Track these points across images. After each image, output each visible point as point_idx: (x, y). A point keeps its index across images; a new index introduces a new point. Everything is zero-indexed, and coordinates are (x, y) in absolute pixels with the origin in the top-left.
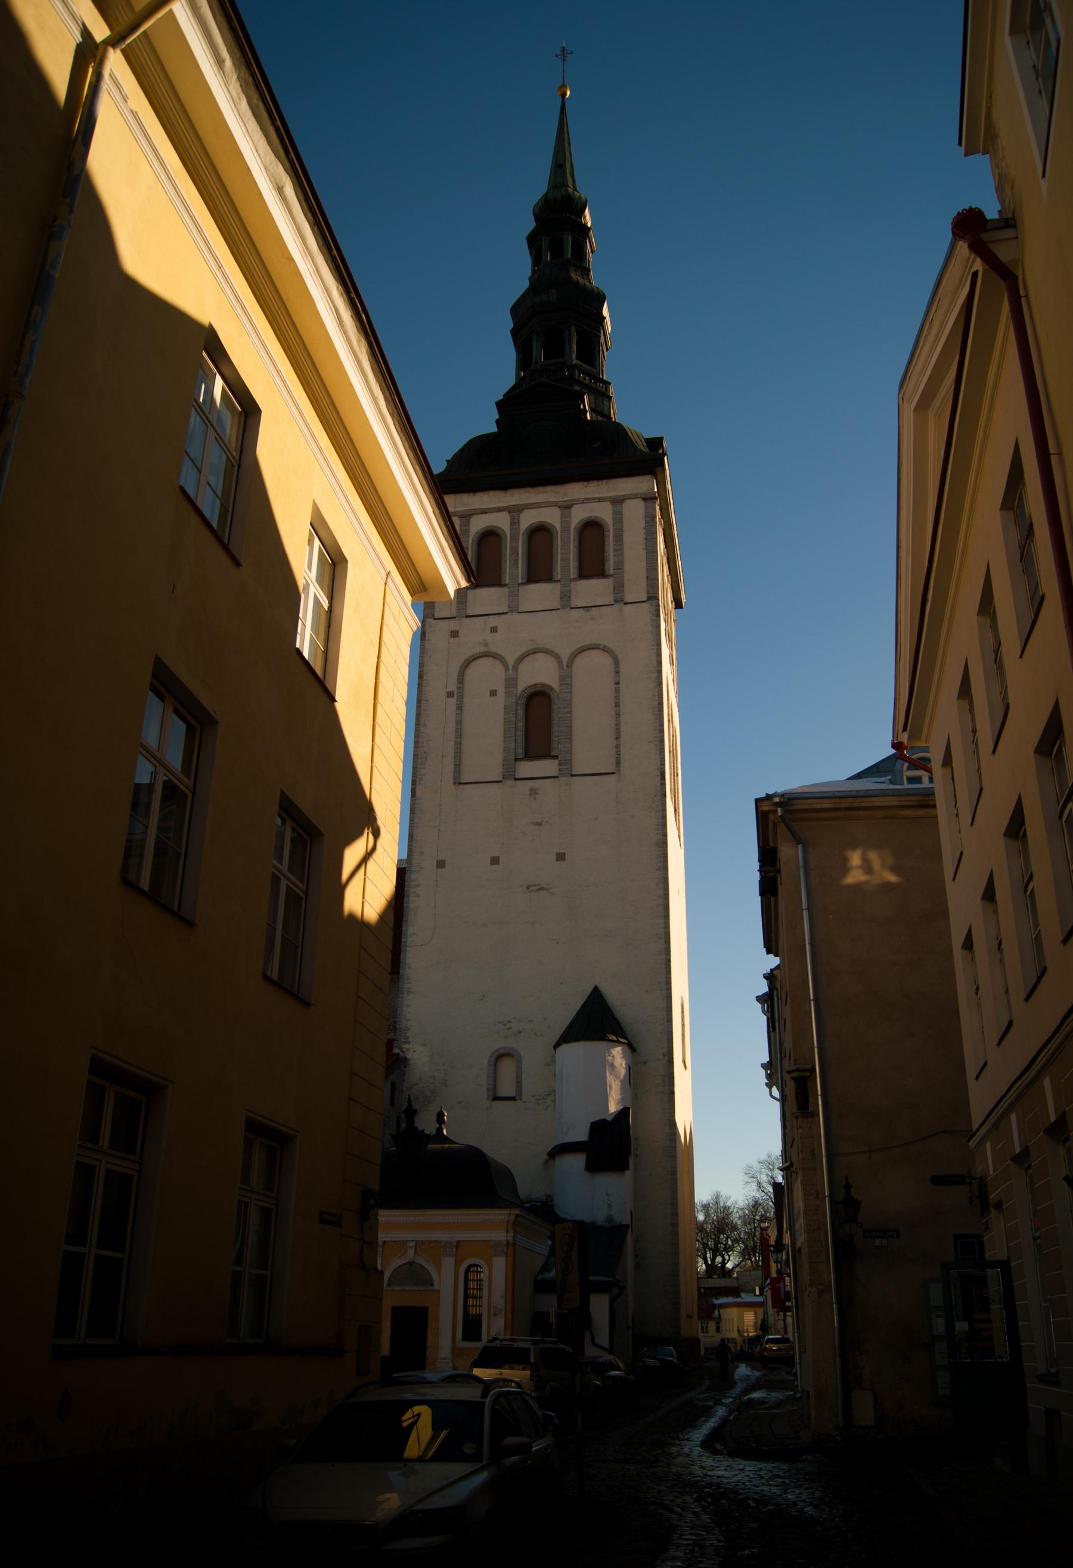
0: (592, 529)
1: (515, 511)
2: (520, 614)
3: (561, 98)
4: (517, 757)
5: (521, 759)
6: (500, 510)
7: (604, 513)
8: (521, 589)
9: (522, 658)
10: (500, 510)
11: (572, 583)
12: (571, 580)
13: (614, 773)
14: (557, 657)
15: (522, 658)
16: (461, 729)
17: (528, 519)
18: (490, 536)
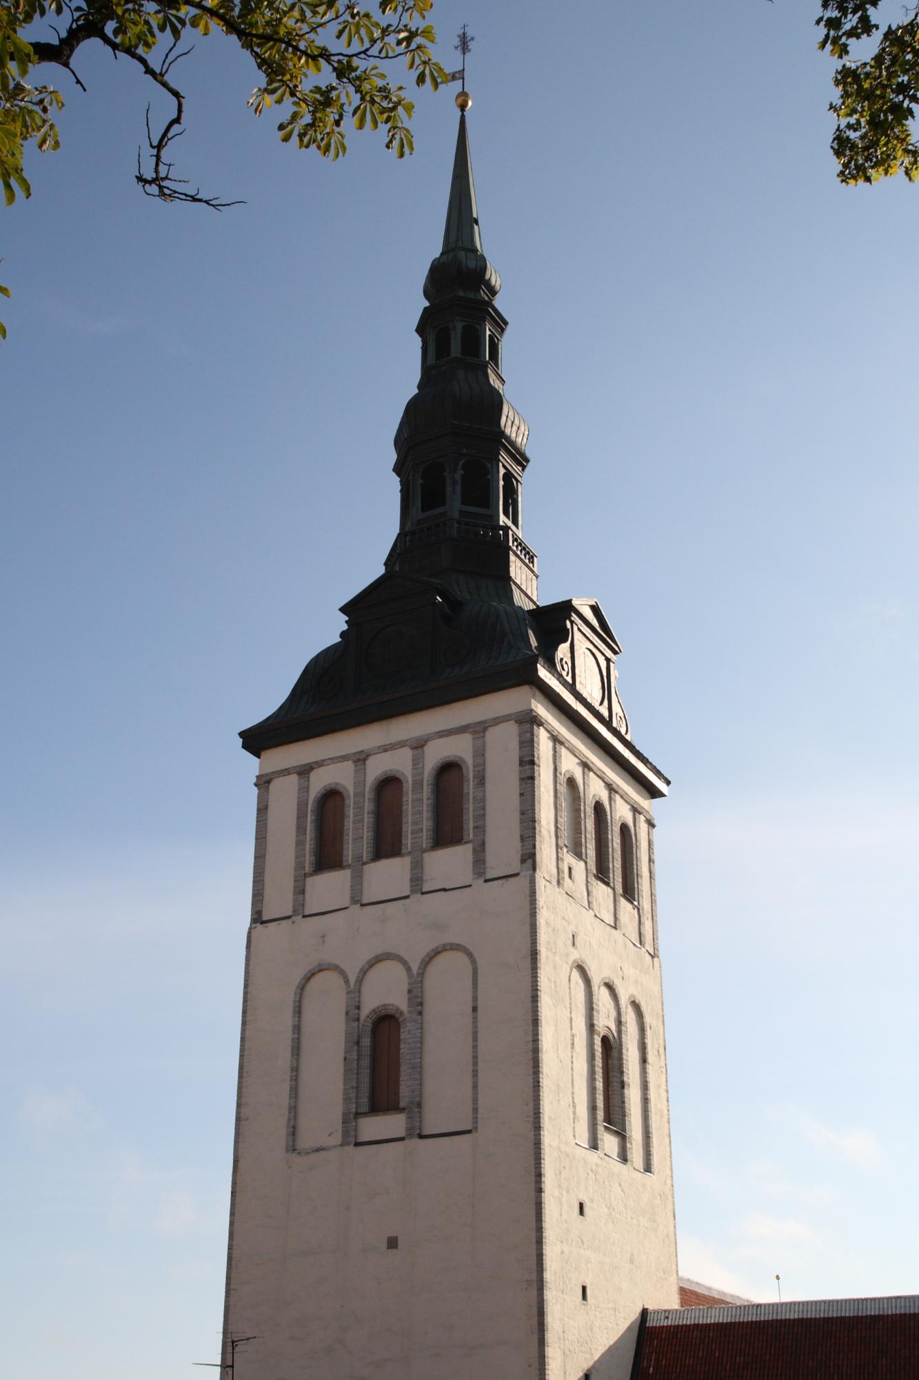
0: (449, 770)
1: (361, 759)
2: (365, 908)
3: (459, 110)
4: (359, 1112)
5: (365, 1114)
6: (344, 758)
7: (460, 748)
8: (366, 867)
9: (364, 972)
10: (344, 758)
11: (426, 855)
12: (426, 851)
13: (469, 1132)
14: (404, 963)
15: (364, 972)
16: (297, 1076)
17: (377, 768)
18: (332, 796)
